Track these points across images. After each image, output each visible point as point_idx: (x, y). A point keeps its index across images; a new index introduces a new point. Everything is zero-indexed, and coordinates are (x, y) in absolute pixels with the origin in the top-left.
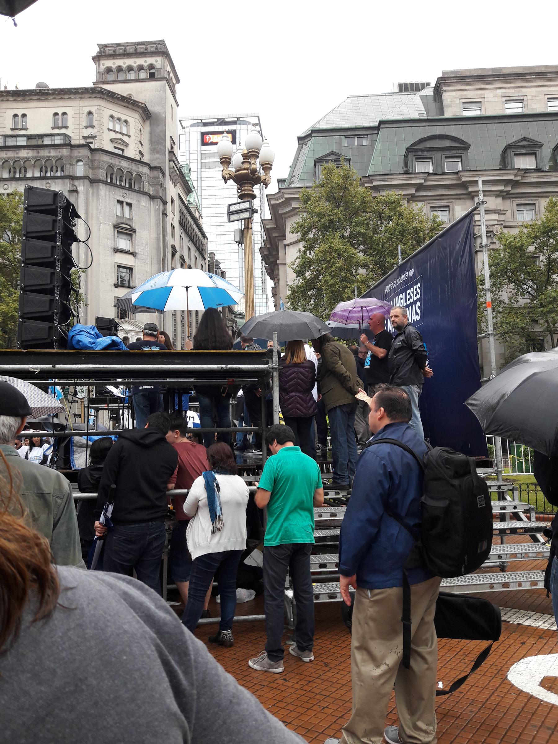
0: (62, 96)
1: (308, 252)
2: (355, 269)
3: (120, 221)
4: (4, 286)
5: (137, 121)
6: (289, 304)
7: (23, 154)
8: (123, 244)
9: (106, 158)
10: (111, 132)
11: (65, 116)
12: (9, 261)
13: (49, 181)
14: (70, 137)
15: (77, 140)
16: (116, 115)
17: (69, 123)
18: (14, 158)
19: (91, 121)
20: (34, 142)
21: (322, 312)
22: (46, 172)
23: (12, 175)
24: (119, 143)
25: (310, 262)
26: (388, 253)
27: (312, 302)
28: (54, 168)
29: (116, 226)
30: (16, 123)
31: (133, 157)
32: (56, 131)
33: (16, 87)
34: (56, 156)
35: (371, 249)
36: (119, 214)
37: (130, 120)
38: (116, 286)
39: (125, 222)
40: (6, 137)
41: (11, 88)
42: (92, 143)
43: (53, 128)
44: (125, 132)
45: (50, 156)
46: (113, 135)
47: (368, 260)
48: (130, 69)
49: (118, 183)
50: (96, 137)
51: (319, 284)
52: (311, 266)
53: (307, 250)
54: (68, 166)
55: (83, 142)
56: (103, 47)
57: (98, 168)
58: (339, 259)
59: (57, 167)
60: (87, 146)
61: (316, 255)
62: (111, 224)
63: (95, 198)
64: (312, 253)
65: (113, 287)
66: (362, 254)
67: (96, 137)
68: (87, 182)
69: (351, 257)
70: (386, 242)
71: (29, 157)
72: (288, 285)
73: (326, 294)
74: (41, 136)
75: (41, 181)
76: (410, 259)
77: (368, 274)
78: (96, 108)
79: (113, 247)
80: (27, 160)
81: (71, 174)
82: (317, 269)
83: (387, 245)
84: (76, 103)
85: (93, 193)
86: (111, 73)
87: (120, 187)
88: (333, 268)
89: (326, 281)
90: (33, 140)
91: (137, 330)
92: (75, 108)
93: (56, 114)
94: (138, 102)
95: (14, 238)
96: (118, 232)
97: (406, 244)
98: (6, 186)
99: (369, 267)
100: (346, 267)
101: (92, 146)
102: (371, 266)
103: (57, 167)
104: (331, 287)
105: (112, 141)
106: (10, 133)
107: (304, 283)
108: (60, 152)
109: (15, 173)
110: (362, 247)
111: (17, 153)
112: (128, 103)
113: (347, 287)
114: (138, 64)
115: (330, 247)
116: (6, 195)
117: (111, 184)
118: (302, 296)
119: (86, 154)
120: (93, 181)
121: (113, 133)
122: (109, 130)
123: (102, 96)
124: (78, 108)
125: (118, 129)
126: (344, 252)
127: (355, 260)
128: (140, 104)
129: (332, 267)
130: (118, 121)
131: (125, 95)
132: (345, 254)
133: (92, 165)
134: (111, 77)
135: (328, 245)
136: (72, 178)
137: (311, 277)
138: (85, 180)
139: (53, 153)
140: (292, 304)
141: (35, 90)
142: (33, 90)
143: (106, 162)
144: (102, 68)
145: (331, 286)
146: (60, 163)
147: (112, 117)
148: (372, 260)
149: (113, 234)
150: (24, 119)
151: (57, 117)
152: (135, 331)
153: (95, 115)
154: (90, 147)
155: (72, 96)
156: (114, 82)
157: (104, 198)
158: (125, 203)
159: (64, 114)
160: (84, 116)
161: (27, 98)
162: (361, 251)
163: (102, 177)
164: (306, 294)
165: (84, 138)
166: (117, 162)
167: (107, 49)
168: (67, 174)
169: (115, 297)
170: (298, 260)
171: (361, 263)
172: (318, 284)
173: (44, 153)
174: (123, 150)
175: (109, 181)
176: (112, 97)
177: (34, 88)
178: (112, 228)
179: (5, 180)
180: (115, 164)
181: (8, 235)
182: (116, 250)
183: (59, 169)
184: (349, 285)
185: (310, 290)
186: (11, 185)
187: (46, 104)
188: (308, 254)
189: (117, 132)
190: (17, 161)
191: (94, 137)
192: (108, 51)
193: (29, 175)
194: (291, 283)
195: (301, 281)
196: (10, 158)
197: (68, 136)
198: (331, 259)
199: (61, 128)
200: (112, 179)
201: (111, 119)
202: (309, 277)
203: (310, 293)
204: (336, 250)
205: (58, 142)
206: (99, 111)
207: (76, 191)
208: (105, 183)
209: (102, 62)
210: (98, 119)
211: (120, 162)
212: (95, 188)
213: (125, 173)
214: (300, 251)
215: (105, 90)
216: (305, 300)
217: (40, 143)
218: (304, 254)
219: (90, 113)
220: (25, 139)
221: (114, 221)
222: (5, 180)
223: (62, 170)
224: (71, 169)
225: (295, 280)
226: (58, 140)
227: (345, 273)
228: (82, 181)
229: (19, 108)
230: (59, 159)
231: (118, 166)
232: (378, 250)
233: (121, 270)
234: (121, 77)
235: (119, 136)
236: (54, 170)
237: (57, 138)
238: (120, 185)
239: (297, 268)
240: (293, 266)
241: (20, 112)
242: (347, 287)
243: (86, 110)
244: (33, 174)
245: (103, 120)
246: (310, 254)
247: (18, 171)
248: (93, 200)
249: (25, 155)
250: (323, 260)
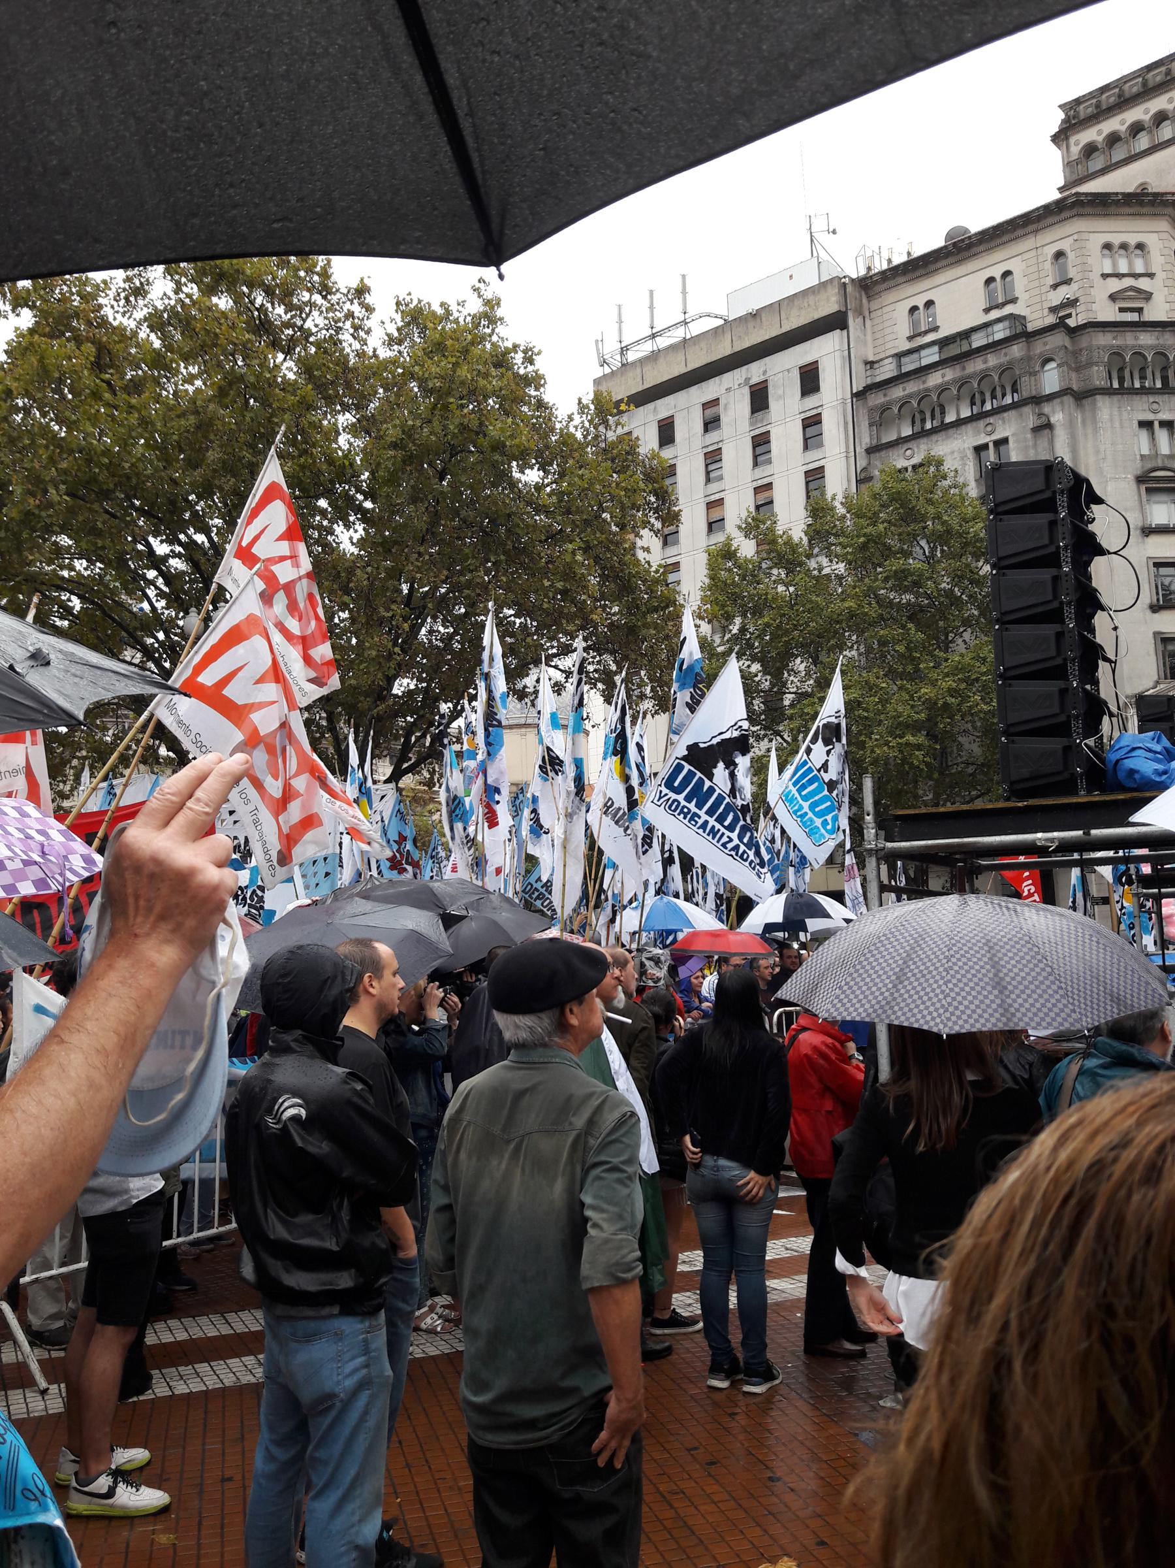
0: (999, 241)
3: (1149, 465)
4: (924, 648)
5: (1165, 236)
7: (935, 379)
9: (1104, 339)
10: (1109, 279)
11: (1008, 279)
12: (929, 597)
13: (991, 420)
14: (1024, 317)
15: (1038, 318)
16: (1116, 240)
17: (1019, 291)
18: (919, 392)
19: (1063, 270)
20: (954, 350)
22: (983, 402)
23: (918, 428)
24: (1130, 298)
28: (998, 389)
29: (1140, 480)
30: (915, 324)
31: (1164, 318)
32: (995, 314)
33: (909, 254)
34: (1001, 365)
36: (1145, 451)
37: (1151, 240)
38: (1155, 608)
39: (1160, 464)
40: (899, 356)
41: (899, 259)
42: (1069, 316)
43: (987, 311)
44: (1139, 269)
45: (987, 369)
46: (1115, 285)
48: (1137, 129)
49: (1137, 385)
50: (1077, 300)
54: (1025, 379)
55: (1051, 319)
56: (1071, 108)
57: (1090, 364)
59: (1003, 387)
60: (1061, 324)
62: (1130, 477)
63: (1090, 431)
65: (1148, 612)
67: (1077, 300)
68: (1068, 400)
71: (947, 383)
74: (966, 334)
75: (974, 424)
78: (1071, 240)
79: (1140, 524)
80: (943, 389)
81: (1034, 393)
84: (1029, 243)
85: (1084, 422)
86: (1094, 155)
87: (1144, 391)
90: (951, 346)
92: (1025, 256)
93: (990, 281)
94: (1163, 194)
95: (933, 550)
96: (1148, 490)
98: (909, 452)
101: (1071, 323)
103: (1003, 387)
105: (1113, 297)
106: (907, 346)
108: (1006, 355)
109: (923, 421)
111: (924, 382)
112: (1141, 204)
114: (1152, 113)
116: (910, 469)
117: (1123, 391)
119: (1061, 343)
120: (1082, 396)
121: (1114, 279)
122: (1105, 276)
123: (1081, 210)
124: (1033, 253)
125: (1123, 268)
128: (1169, 197)
130: (1122, 252)
131: (1130, 190)
133: (1076, 362)
134: (1097, 163)
136: (1038, 400)
138: (1065, 398)
139: (993, 360)
141: (945, 247)
142: (941, 249)
143: (1105, 347)
144: (1075, 150)
146: (1010, 378)
147: (1107, 246)
149: (1136, 498)
150: (931, 310)
151: (992, 285)
153: (1071, 255)
154: (1067, 327)
155: (1020, 232)
156: (1104, 171)
157: (1109, 424)
158: (1156, 424)
159: (1007, 274)
160: (1048, 265)
161: (932, 267)
163: (1099, 381)
165: (1053, 310)
166: (1129, 339)
167: (1082, 107)
168: (1025, 394)
169: (1156, 634)
173: (976, 366)
174: (1140, 310)
175: (1116, 385)
176: (1103, 205)
177: (941, 243)
178: (1133, 485)
179: (907, 439)
180: (1127, 346)
181: (922, 547)
182: (1149, 531)
183: (1009, 390)
186: (918, 447)
189: (1124, 275)
190: (924, 396)
191: (1072, 303)
192: (1083, 111)
193: (950, 418)
196: (910, 396)
197: (1019, 316)
199: (1004, 304)
200: (1121, 380)
201: (1106, 252)
205: (999, 336)
206: (1078, 245)
207: (1049, 426)
208: (1108, 392)
209: (1072, 140)
210: (1079, 260)
211: (1136, 338)
212: (1087, 408)
213: (1149, 359)
215: (1086, 194)
217: (965, 348)
219: (1059, 255)
220: (936, 348)
221: (1137, 468)
222: (907, 439)
223: (1014, 390)
224: (1033, 383)
226: (1000, 333)
228: (1058, 400)
229: (916, 293)
230: (1005, 370)
231: (1134, 346)
233: (1163, 571)
234: (1119, 154)
235: (1128, 282)
236: (999, 394)
237: (1000, 326)
238: (1143, 387)
241: (920, 301)
243: (1051, 250)
244: (958, 413)
245: (1090, 260)
247: (928, 415)
248: (1086, 435)
249: (940, 381)
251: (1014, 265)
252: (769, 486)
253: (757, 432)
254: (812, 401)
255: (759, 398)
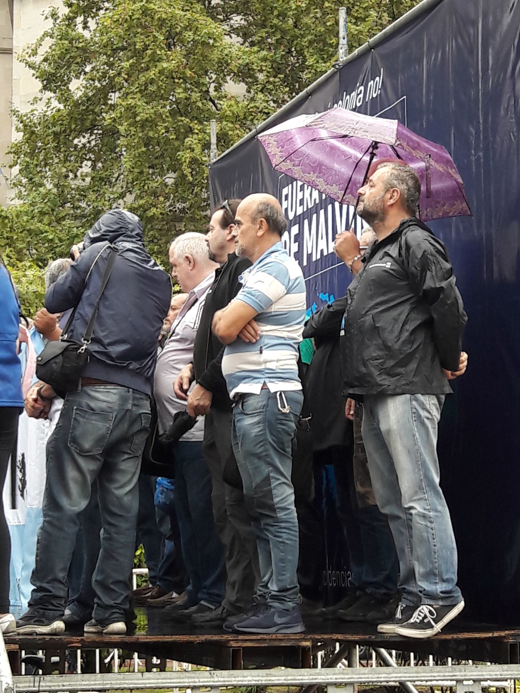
1: (80, 19)
2: (216, 81)
6: (16, 169)
21: (115, 200)
25: (84, 50)
26: (311, 42)
27: (86, 168)
35: (264, 26)
47: (253, 58)
51: (108, 117)
52: (87, 60)
53: (76, 14)
58: (169, 47)
61: (104, 30)
64: (92, 24)
66: (236, 40)
69: (205, 44)
70: (307, 11)
72: (15, 112)
73: (128, 147)
76: (371, 48)
77: (253, 99)
82: (105, 74)
83: (306, 20)
88: (152, 74)
89: (129, 108)
97: (364, 20)
99: (256, 80)
100: (188, 73)
102: (261, 77)
104: (142, 126)
107: (65, 112)
110: (237, 20)
113: (191, 130)
115: (145, 12)
118: (57, 149)
126: (185, 28)
127: (215, 55)
129: (148, 69)
132: (189, 35)
135: (138, 5)
137: (85, 95)
140: (26, 170)
145: (145, 124)
148: (265, 59)
162: (235, 30)
164: (68, 143)
170: (48, 42)
171: (234, 65)
172: (107, 116)
184: (197, 127)
185: (79, 133)
188: (80, 27)
194: (24, 109)
195: (55, 103)
198: (146, 47)
202: (80, 93)
203: (80, 141)
204: (162, 22)
214: (54, 16)
216: (66, 160)
218: (68, 25)
225: (36, 100)
227: (186, 90)
232: (284, 32)
239: (45, 66)
240: (32, 59)
242: (191, 130)
246: (85, 27)
250: (123, 49)
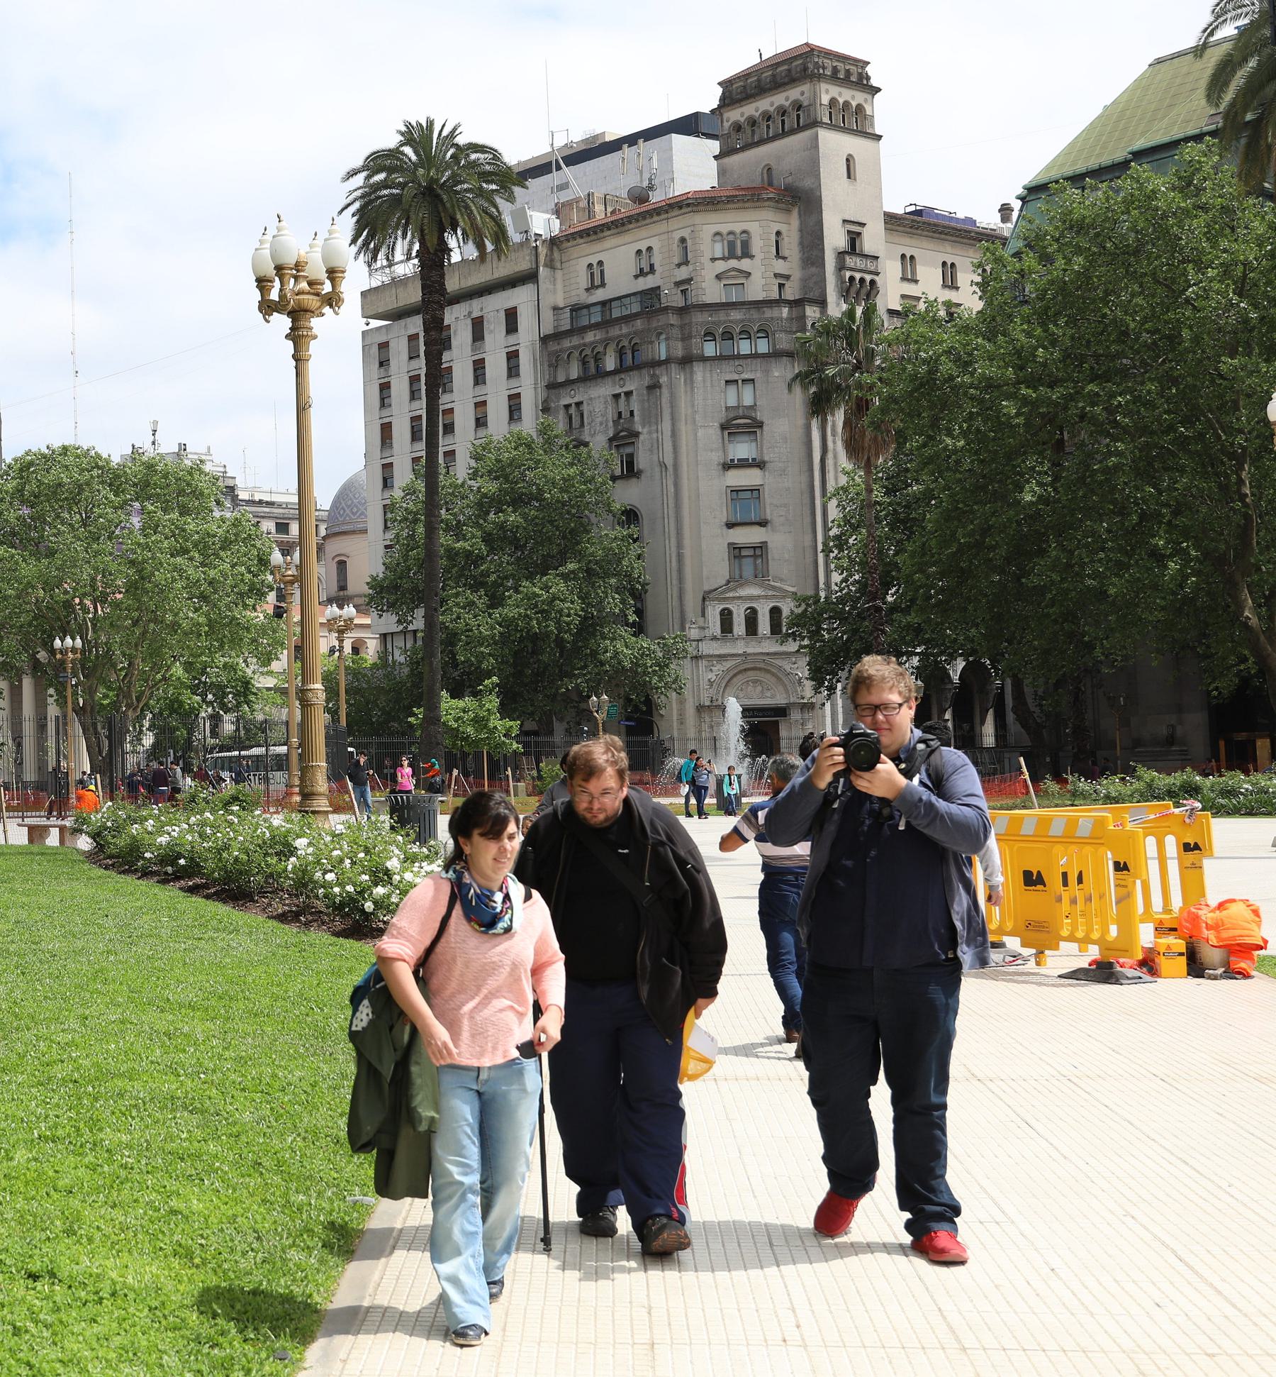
8: (742, 449)
24: (734, 277)
29: (723, 427)
84: (662, 227)
91: (770, 593)
105: (718, 277)
124: (665, 236)
152: (766, 597)
153: (689, 243)
159: (649, 249)
178: (719, 432)
182: (728, 466)
187: (627, 237)
219: (683, 240)
221: (722, 416)
243: (677, 235)
251: (655, 243)
252: (484, 403)
253: (477, 358)
254: (512, 339)
255: (478, 328)
